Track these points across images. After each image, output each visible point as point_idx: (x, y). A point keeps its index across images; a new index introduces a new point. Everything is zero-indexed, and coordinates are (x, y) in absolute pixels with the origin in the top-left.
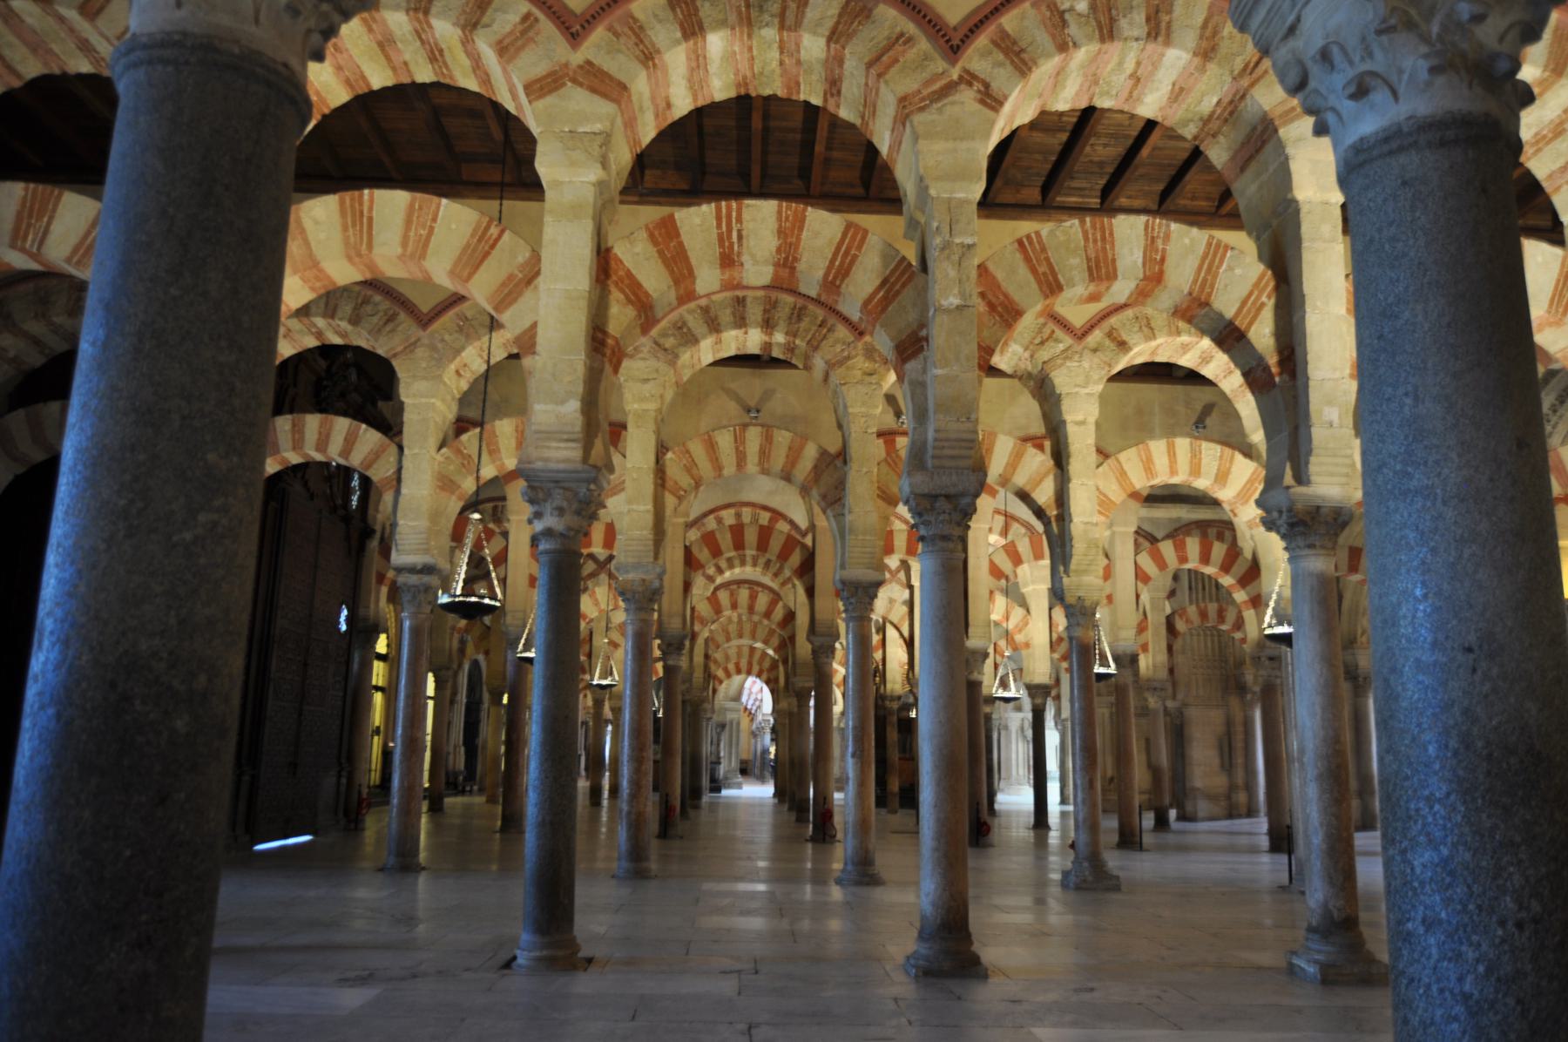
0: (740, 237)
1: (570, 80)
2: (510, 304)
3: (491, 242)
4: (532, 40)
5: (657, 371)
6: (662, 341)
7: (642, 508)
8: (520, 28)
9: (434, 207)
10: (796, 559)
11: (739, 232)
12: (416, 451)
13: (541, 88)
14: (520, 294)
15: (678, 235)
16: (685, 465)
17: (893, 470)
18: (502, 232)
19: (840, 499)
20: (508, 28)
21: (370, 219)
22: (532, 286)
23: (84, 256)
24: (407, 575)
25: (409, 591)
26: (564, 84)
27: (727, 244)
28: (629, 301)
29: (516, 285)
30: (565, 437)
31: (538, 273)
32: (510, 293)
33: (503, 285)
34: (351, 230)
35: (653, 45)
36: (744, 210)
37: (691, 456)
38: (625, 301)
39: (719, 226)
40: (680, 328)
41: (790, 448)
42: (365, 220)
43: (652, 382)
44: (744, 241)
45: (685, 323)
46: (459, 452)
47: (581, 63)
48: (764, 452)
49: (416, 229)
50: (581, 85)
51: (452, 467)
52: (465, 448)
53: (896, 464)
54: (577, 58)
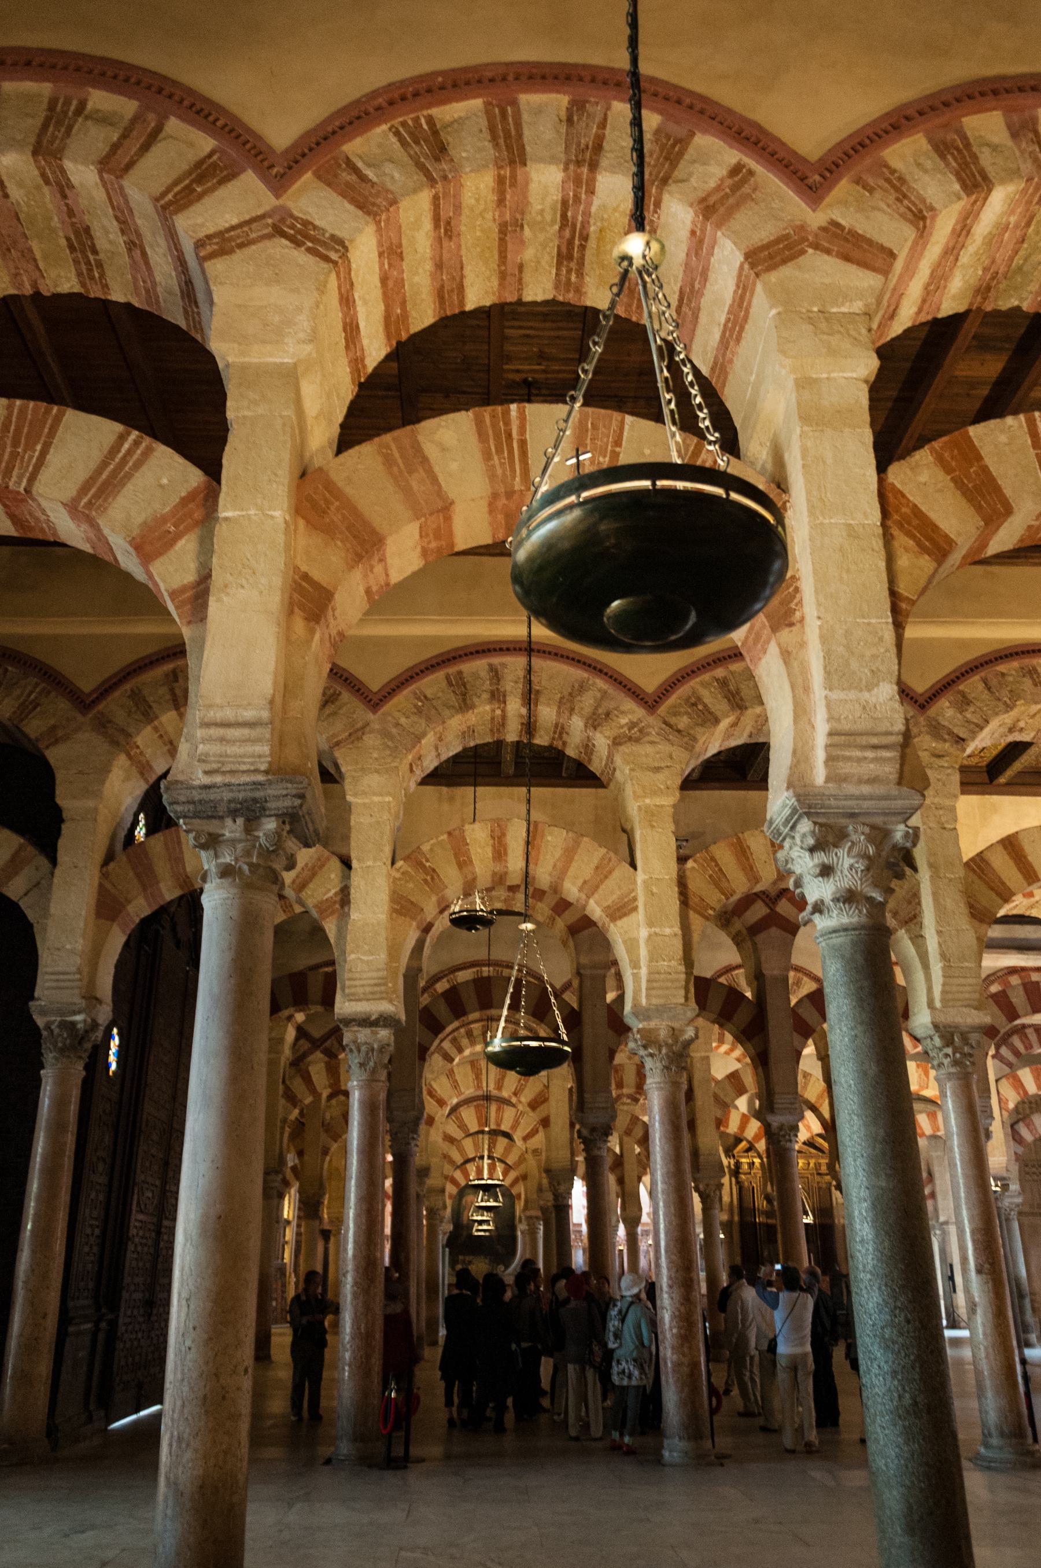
1: (811, 246)
4: (748, 197)
5: (671, 757)
6: (673, 720)
7: (668, 931)
8: (729, 182)
9: (614, 425)
12: (370, 863)
13: (771, 257)
15: (979, 458)
16: (711, 876)
17: (980, 877)
19: (915, 916)
20: (712, 184)
21: (523, 443)
23: (97, 496)
24: (356, 1028)
26: (803, 252)
28: (924, 549)
34: (496, 458)
35: (923, 201)
37: (717, 865)
38: (916, 549)
40: (694, 705)
42: (515, 445)
43: (666, 772)
45: (699, 699)
47: (824, 224)
50: (828, 252)
51: (411, 885)
53: (982, 871)
54: (816, 219)
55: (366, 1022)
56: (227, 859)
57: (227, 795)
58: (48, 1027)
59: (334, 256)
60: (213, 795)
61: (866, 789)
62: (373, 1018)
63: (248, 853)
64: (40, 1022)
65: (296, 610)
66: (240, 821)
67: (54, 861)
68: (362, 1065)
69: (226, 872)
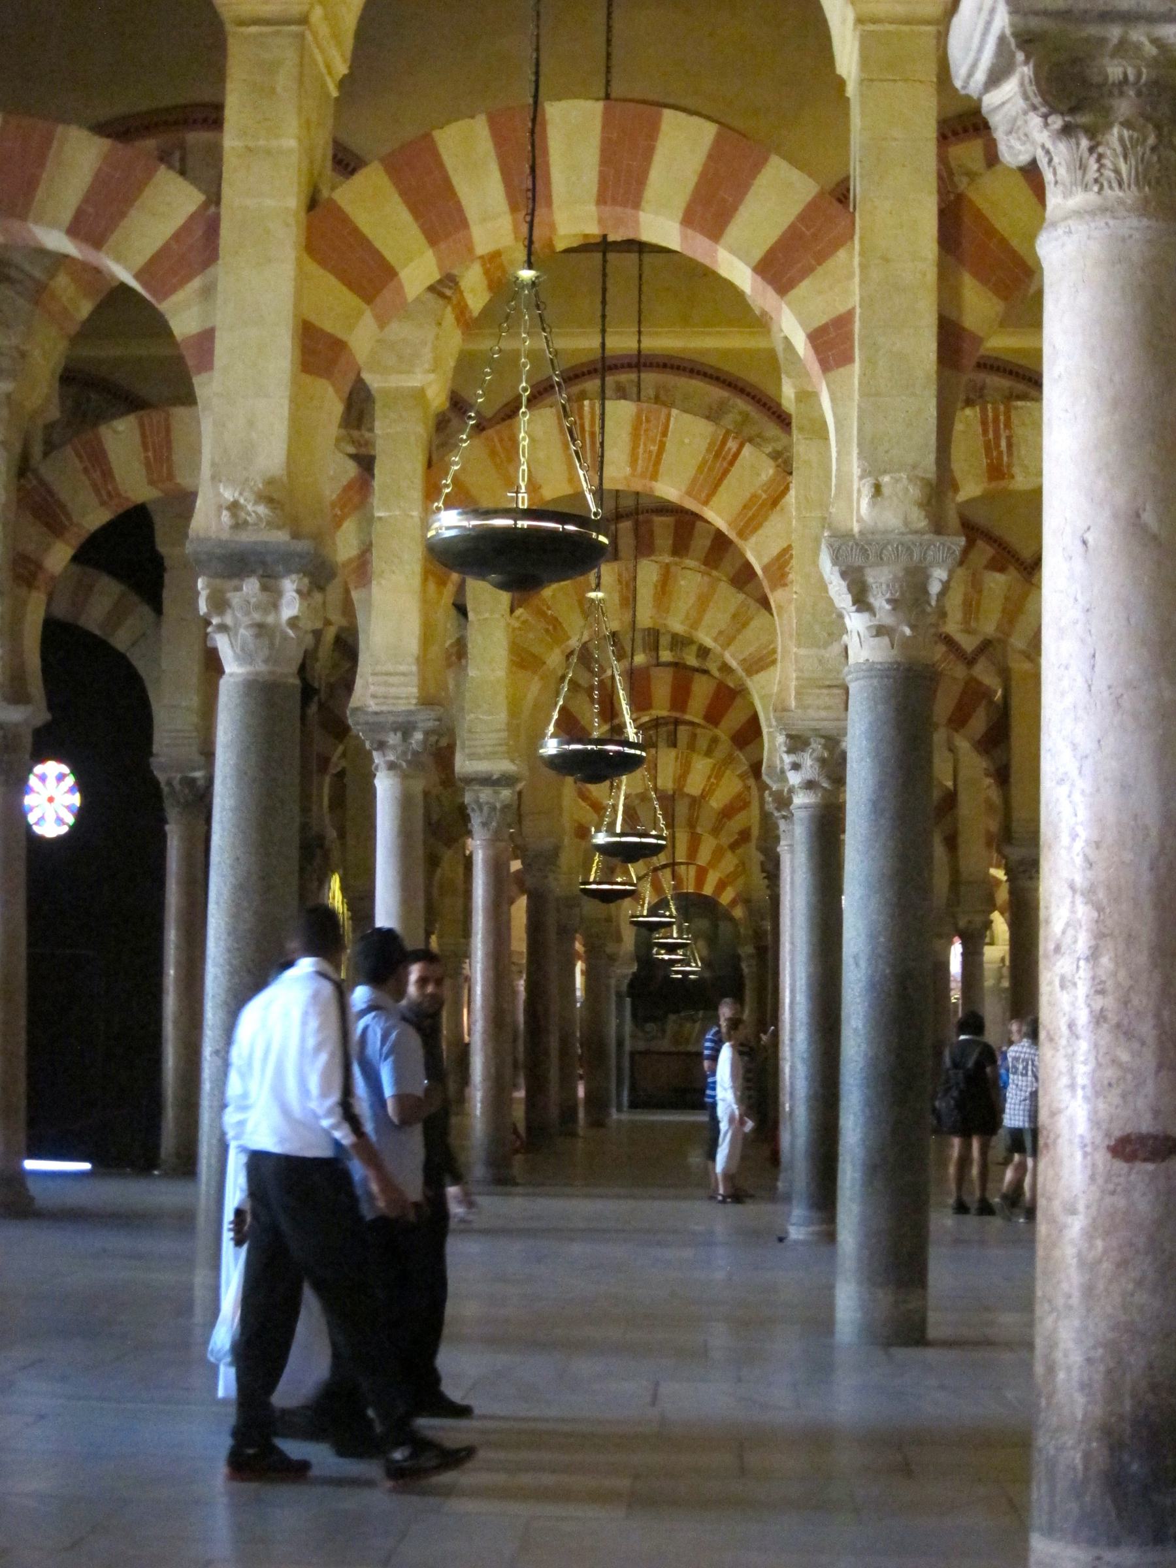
0: (1010, 445)
2: (755, 530)
3: (730, 457)
10: (979, 723)
11: (1009, 439)
12: (487, 615)
14: (766, 518)
18: (741, 446)
22: (778, 508)
24: (476, 787)
25: (481, 810)
27: (995, 454)
29: (762, 505)
30: (828, 683)
31: (787, 489)
32: (751, 519)
33: (745, 507)
36: (1013, 414)
39: (985, 432)
41: (1007, 598)
44: (1014, 449)
46: (541, 614)
48: (971, 605)
49: (645, 445)
51: (531, 636)
52: (549, 608)
55: (487, 781)
56: (391, 757)
57: (391, 719)
58: (169, 783)
59: (448, 292)
60: (381, 719)
61: (823, 714)
62: (495, 777)
63: (404, 753)
64: (161, 777)
65: (430, 578)
66: (399, 734)
67: (158, 609)
68: (485, 824)
69: (392, 766)
